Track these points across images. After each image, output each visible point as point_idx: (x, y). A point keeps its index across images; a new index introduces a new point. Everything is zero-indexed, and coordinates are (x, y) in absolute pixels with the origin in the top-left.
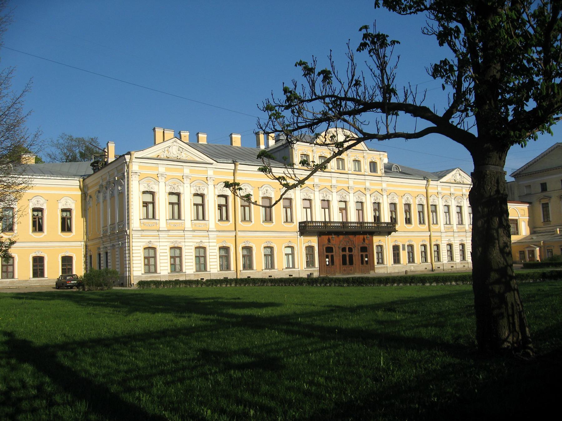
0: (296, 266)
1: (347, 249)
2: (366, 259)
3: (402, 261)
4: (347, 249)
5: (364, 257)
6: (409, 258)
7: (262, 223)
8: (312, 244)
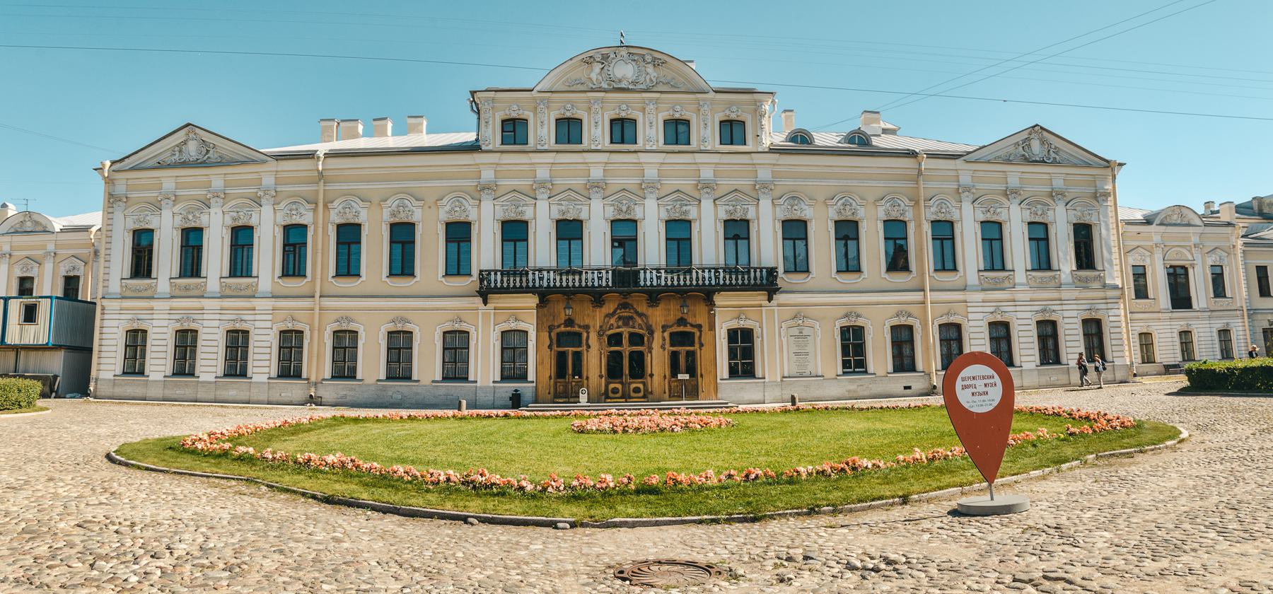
3: (871, 366)
7: (384, 278)
8: (522, 326)
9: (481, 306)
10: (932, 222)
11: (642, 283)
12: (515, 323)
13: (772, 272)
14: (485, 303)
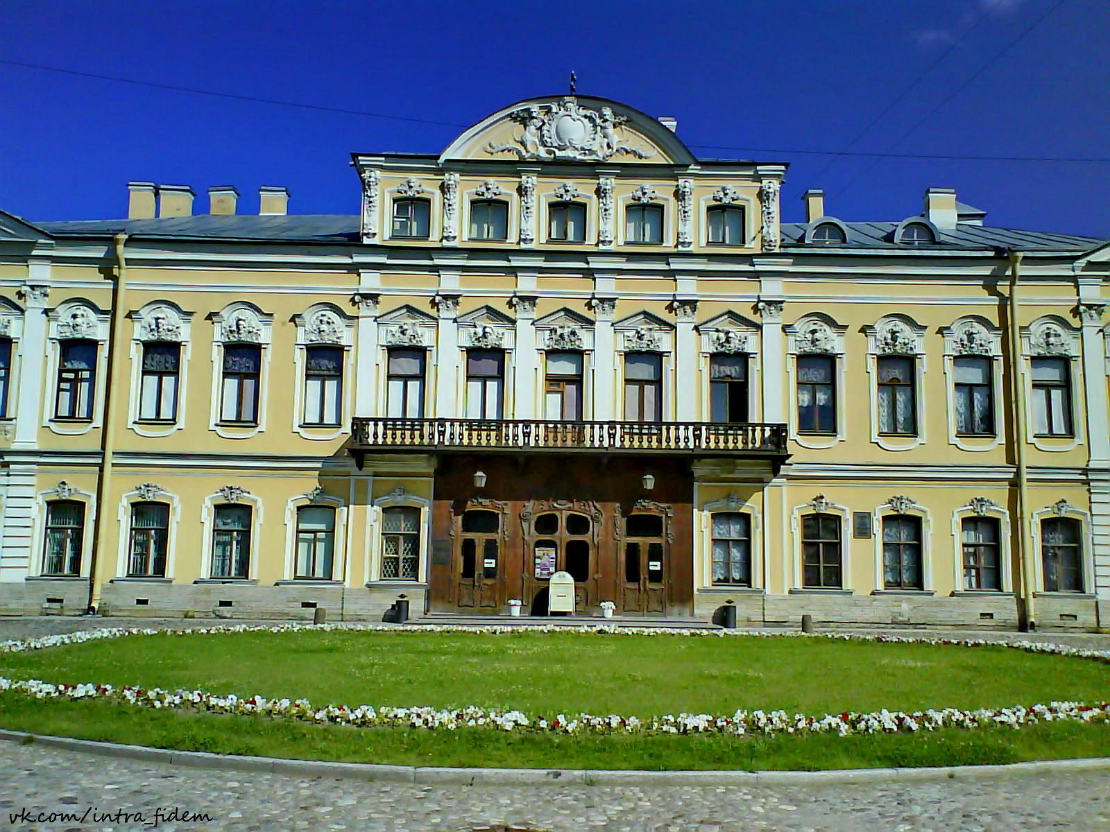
0: (337, 575)
1: (562, 523)
2: (655, 566)
4: (562, 523)
5: (644, 557)
6: (894, 568)
8: (413, 501)
9: (355, 470)
10: (1033, 358)
11: (588, 444)
12: (403, 496)
13: (779, 431)
14: (360, 465)
